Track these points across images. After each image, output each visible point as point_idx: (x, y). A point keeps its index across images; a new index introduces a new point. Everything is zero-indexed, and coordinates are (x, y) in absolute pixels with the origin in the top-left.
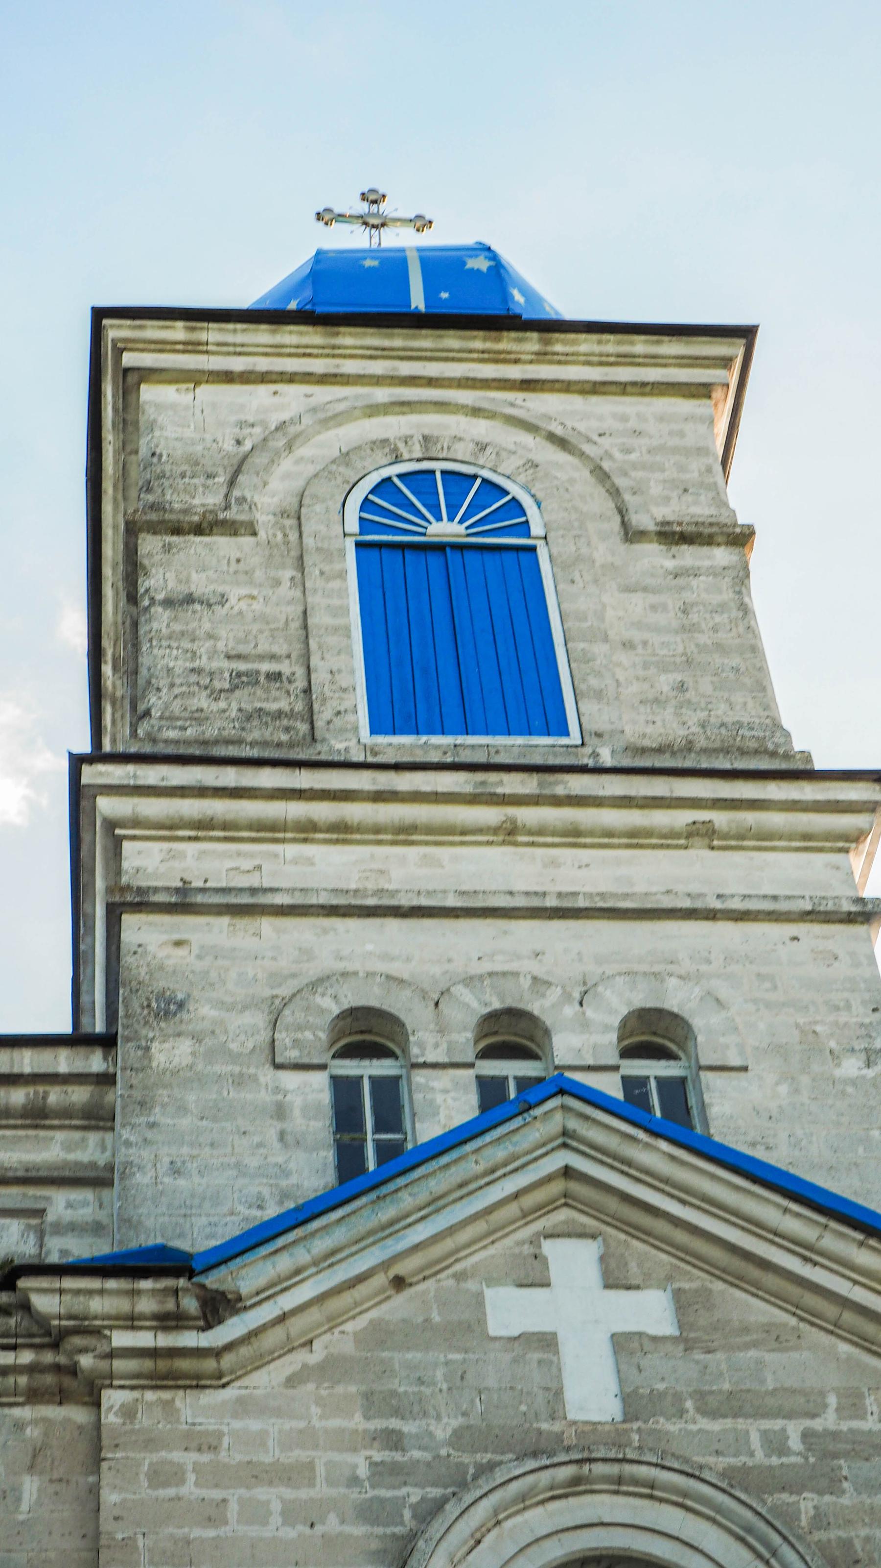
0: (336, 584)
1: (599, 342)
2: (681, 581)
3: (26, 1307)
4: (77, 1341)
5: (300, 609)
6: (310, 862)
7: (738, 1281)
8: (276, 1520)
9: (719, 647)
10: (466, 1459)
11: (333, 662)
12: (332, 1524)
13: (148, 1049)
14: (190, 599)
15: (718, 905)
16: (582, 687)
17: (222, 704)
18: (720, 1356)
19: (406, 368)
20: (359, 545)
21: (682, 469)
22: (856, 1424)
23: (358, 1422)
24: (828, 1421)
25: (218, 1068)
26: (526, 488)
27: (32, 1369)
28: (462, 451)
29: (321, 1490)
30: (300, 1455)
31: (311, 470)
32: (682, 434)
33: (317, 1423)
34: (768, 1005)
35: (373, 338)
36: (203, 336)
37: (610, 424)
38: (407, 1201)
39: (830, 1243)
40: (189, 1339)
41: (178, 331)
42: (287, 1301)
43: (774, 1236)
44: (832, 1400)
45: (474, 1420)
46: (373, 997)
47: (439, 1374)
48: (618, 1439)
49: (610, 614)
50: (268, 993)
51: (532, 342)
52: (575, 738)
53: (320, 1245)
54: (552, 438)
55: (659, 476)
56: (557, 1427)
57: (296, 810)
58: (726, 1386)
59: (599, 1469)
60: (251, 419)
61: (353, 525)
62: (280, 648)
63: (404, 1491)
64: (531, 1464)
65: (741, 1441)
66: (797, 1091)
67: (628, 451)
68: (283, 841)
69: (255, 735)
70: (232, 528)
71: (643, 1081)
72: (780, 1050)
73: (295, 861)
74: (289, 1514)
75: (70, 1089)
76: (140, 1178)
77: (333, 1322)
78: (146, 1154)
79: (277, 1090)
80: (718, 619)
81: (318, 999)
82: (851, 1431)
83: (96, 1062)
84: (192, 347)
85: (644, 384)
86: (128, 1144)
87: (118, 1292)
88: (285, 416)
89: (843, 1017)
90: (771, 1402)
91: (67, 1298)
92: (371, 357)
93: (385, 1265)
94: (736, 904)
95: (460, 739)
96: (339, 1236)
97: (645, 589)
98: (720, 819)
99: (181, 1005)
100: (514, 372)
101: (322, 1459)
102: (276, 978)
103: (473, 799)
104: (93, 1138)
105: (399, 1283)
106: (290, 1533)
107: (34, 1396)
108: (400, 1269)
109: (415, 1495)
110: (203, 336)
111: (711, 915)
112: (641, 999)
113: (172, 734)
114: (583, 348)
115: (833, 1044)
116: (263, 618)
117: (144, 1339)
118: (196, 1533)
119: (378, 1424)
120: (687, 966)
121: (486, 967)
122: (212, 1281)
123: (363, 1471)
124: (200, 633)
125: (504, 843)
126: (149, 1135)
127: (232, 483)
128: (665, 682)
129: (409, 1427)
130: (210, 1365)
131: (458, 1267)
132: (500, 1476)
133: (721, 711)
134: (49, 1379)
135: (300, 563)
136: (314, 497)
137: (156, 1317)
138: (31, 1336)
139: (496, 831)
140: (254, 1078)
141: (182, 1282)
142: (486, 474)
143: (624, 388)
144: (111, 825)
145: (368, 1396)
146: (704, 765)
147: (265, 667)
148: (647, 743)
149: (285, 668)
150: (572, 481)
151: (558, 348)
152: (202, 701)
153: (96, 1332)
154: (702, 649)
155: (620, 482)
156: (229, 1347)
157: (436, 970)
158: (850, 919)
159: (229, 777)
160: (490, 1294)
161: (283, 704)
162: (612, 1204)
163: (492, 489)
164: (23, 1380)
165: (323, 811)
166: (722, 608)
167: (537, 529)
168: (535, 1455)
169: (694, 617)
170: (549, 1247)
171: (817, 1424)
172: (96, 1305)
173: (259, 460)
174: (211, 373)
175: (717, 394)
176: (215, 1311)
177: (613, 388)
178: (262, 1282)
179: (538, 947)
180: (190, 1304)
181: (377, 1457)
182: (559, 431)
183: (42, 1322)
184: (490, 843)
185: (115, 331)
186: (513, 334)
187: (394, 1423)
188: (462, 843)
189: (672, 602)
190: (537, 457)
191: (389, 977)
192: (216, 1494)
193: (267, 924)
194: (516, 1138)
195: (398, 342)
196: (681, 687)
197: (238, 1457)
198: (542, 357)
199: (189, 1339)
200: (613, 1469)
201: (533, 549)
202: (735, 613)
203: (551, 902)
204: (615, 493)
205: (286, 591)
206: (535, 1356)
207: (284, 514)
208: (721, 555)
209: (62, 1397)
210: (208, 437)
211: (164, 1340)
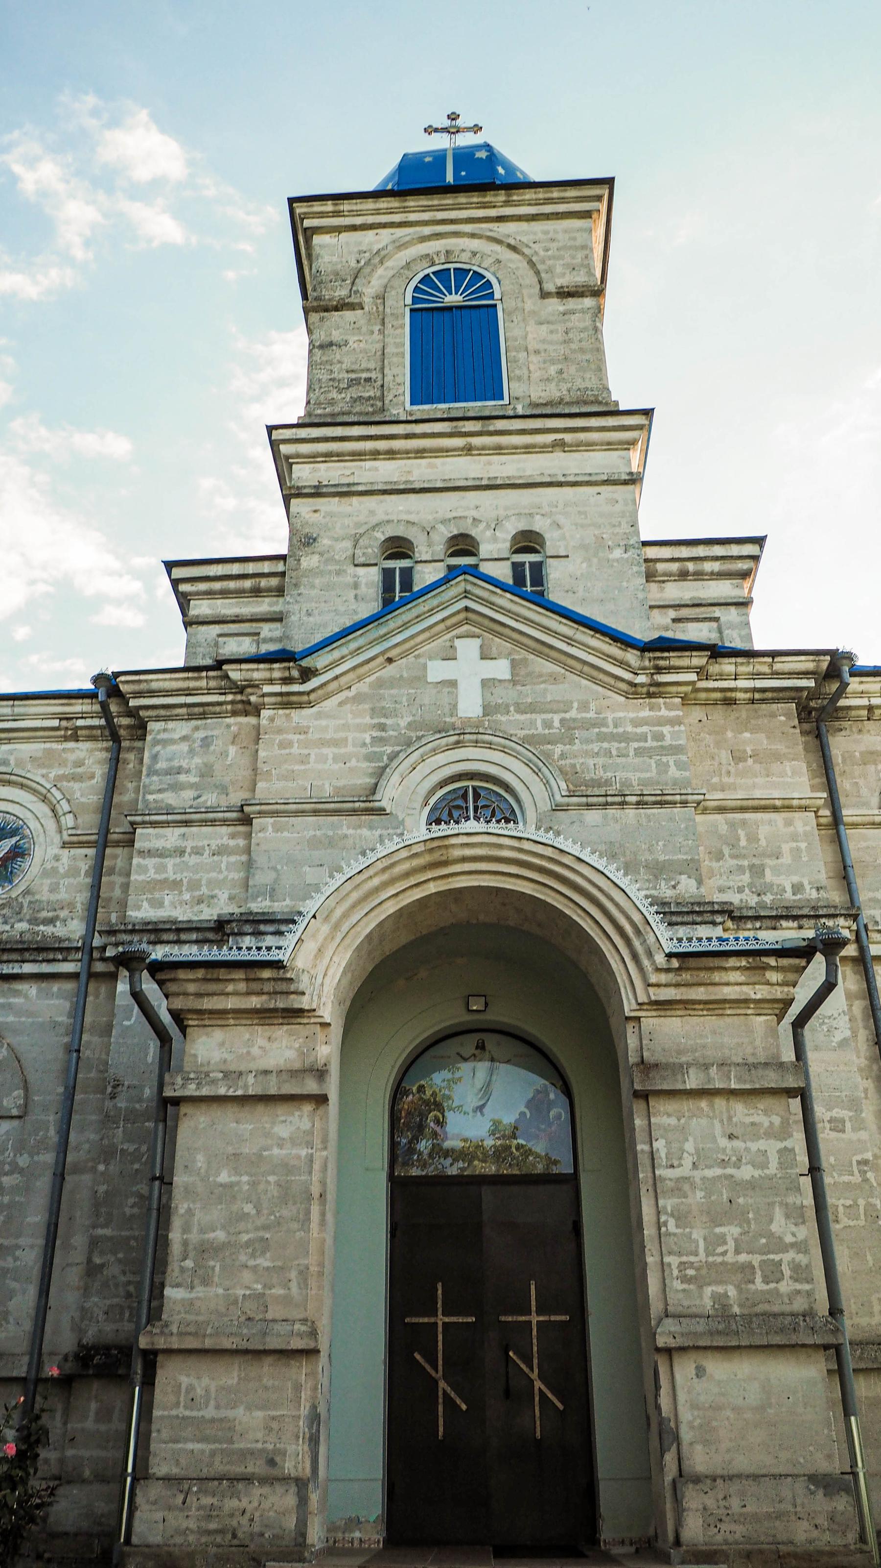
0: (399, 331)
1: (535, 193)
2: (566, 317)
3: (227, 677)
4: (249, 690)
5: (379, 346)
6: (377, 469)
7: (539, 654)
8: (330, 761)
9: (582, 350)
10: (413, 734)
11: (395, 371)
12: (353, 763)
13: (299, 560)
14: (331, 344)
15: (563, 479)
16: (512, 375)
17: (343, 395)
18: (528, 687)
19: (440, 215)
20: (411, 310)
21: (573, 257)
22: (584, 715)
23: (367, 720)
24: (573, 714)
25: (330, 568)
26: (494, 274)
27: (232, 702)
28: (465, 257)
29: (350, 749)
30: (342, 735)
31: (391, 273)
32: (574, 239)
33: (350, 721)
34: (582, 526)
35: (424, 201)
36: (341, 208)
37: (540, 236)
38: (392, 625)
39: (579, 636)
40: (296, 688)
41: (329, 207)
42: (338, 671)
43: (555, 634)
44: (575, 705)
45: (417, 718)
46: (400, 531)
47: (404, 699)
48: (479, 724)
49: (530, 336)
50: (353, 532)
51: (501, 196)
52: (506, 401)
53: (353, 646)
54: (509, 246)
55: (561, 262)
56: (453, 720)
57: (369, 445)
58: (529, 700)
59: (467, 737)
60: (364, 249)
61: (409, 301)
62: (372, 365)
63: (385, 748)
64: (438, 736)
65: (533, 723)
66: (590, 566)
67: (547, 250)
68: (365, 460)
69: (357, 409)
70: (352, 307)
71: (523, 564)
72: (584, 547)
73: (369, 470)
74: (335, 759)
75: (270, 579)
76: (294, 618)
77: (360, 679)
78: (296, 607)
79: (355, 576)
80: (582, 335)
81: (375, 534)
82: (582, 718)
84: (337, 214)
85: (557, 214)
86: (288, 603)
87: (264, 670)
88: (380, 246)
89: (617, 530)
90: (548, 706)
91: (243, 672)
92: (423, 211)
93: (383, 653)
94: (571, 479)
95: (452, 405)
96: (361, 641)
97: (548, 323)
98: (568, 437)
99: (315, 540)
100: (493, 213)
101: (351, 736)
102: (358, 525)
103: (451, 435)
105: (390, 660)
106: (336, 767)
107: (234, 713)
108: (391, 654)
109: (389, 750)
110: (341, 208)
111: (560, 484)
112: (522, 526)
113: (319, 412)
114: (527, 197)
115: (610, 543)
116: (365, 351)
117: (277, 688)
118: (296, 767)
119: (376, 721)
120: (546, 509)
121: (454, 514)
122: (304, 663)
123: (368, 740)
124: (335, 361)
125: (466, 455)
126: (298, 598)
127: (353, 283)
128: (553, 370)
129: (389, 722)
130: (305, 698)
131: (416, 653)
132: (424, 741)
133: (579, 383)
134: (240, 706)
135: (383, 324)
136: (392, 287)
137: (281, 679)
138: (231, 689)
139: (462, 449)
140: (345, 571)
141: (291, 664)
142: (475, 268)
143: (548, 217)
145: (373, 709)
146: (567, 411)
147: (364, 375)
148: (541, 401)
149: (373, 375)
150: (517, 268)
151: (515, 198)
152: (334, 394)
153: (257, 686)
154: (573, 351)
155: (540, 267)
156: (313, 691)
157: (430, 517)
158: (625, 483)
159: (339, 431)
160: (429, 663)
161: (371, 393)
162: (486, 622)
163: (478, 276)
164: (229, 707)
165: (382, 445)
166: (585, 329)
167: (497, 295)
168: (440, 732)
169: (571, 335)
170: (458, 643)
171: (567, 716)
172: (256, 675)
173: (367, 270)
174: (346, 226)
175: (595, 215)
176: (307, 676)
177: (542, 217)
178: (327, 662)
179: (478, 504)
180: (295, 673)
181: (375, 734)
182: (512, 242)
183: (234, 683)
184: (459, 455)
185: (300, 209)
186: (492, 193)
187: (383, 720)
188: (447, 456)
189: (561, 328)
190: (500, 257)
191: (408, 522)
192: (306, 752)
193: (355, 500)
194: (443, 594)
195: (436, 202)
196: (561, 372)
197: (317, 736)
198: (507, 203)
199: (296, 688)
200: (474, 737)
201: (495, 306)
202: (591, 332)
203: (485, 482)
204: (537, 273)
205: (376, 336)
206: (446, 690)
207: (378, 297)
208: (588, 302)
209: (246, 714)
210: (344, 260)
211: (285, 689)
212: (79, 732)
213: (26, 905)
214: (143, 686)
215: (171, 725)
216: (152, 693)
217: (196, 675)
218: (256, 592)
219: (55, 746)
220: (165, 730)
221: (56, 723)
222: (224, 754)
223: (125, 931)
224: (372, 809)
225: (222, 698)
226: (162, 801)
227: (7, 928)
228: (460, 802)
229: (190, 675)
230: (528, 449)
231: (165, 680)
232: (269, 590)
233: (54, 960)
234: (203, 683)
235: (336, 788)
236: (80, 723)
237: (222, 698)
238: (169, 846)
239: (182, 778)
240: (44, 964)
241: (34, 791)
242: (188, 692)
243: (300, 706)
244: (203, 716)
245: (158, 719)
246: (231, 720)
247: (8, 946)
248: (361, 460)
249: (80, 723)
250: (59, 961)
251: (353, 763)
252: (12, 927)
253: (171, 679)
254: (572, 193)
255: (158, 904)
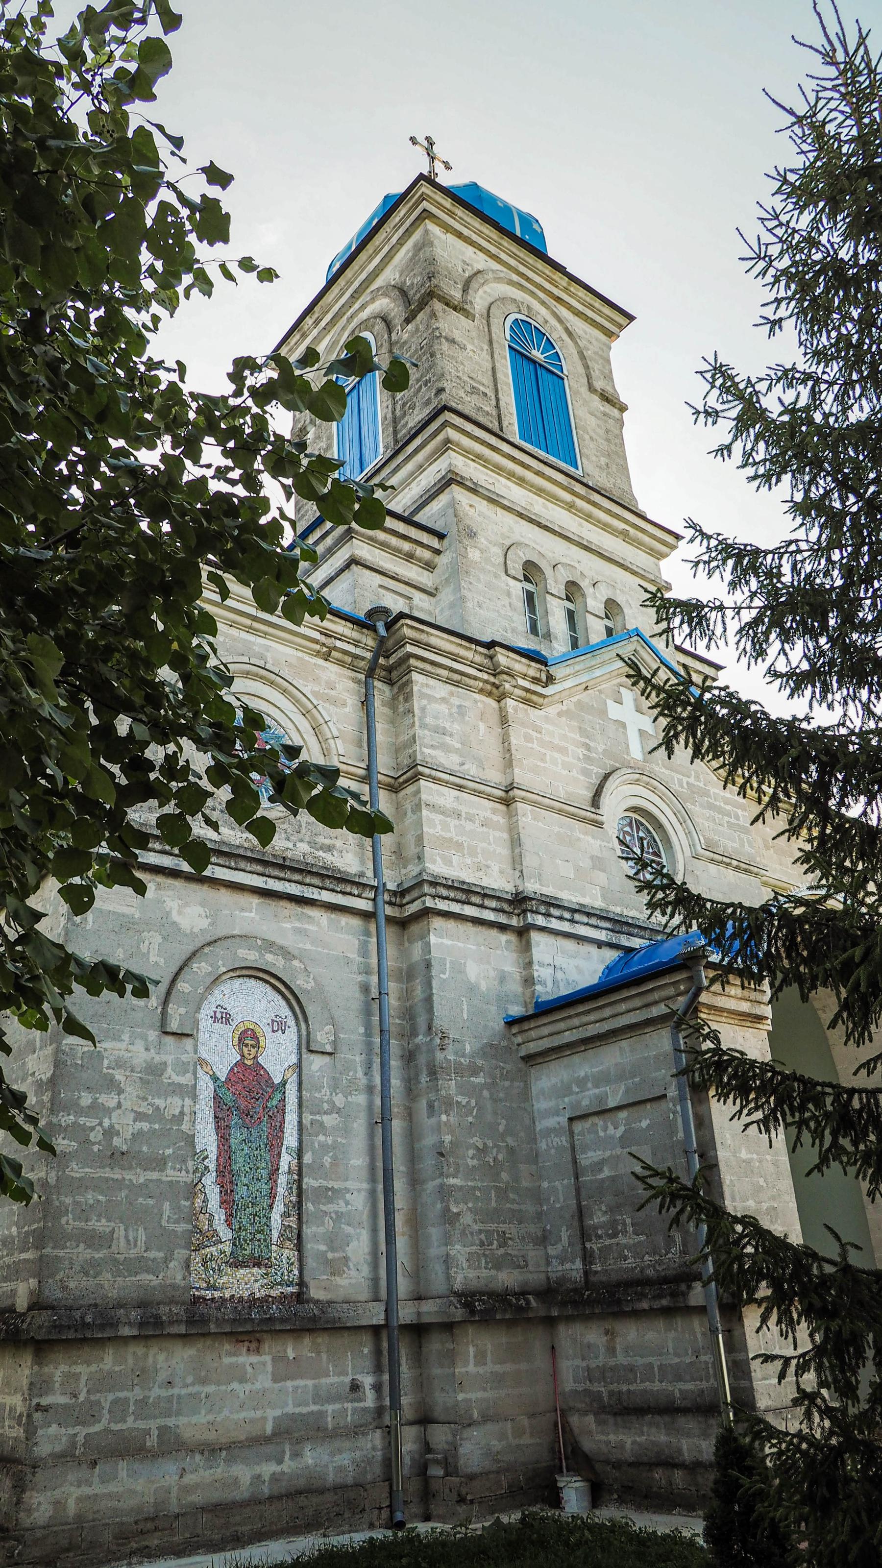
4: (505, 677)
6: (509, 488)
40: (539, 689)
54: (567, 330)
57: (511, 465)
79: (507, 585)
83: (435, 543)
98: (632, 531)
104: (426, 573)
107: (481, 691)
114: (580, 294)
119: (583, 740)
129: (592, 744)
134: (489, 687)
137: (533, 678)
139: (567, 503)
144: (448, 441)
164: (481, 684)
165: (519, 470)
193: (498, 509)
199: (539, 689)
204: (587, 367)
208: (615, 412)
209: (490, 694)
212: (333, 653)
213: (304, 825)
214: (423, 637)
215: (432, 682)
216: (428, 647)
217: (467, 644)
218: (410, 557)
219: (307, 657)
220: (427, 685)
221: (316, 635)
222: (475, 727)
223: (444, 886)
224: (596, 822)
225: (479, 674)
226: (431, 756)
227: (290, 845)
228: (627, 829)
229: (464, 643)
230: (606, 527)
231: (443, 639)
232: (420, 560)
233: (350, 894)
234: (469, 655)
235: (567, 792)
236: (339, 644)
237: (479, 674)
238: (448, 806)
239: (448, 739)
240: (340, 895)
241: (296, 702)
242: (455, 658)
243: (535, 706)
244: (457, 684)
245: (422, 672)
246: (477, 696)
247: (315, 870)
248: (498, 474)
249: (339, 644)
250: (354, 895)
251: (574, 773)
252: (295, 845)
253: (448, 640)
254: (607, 310)
255: (448, 862)
